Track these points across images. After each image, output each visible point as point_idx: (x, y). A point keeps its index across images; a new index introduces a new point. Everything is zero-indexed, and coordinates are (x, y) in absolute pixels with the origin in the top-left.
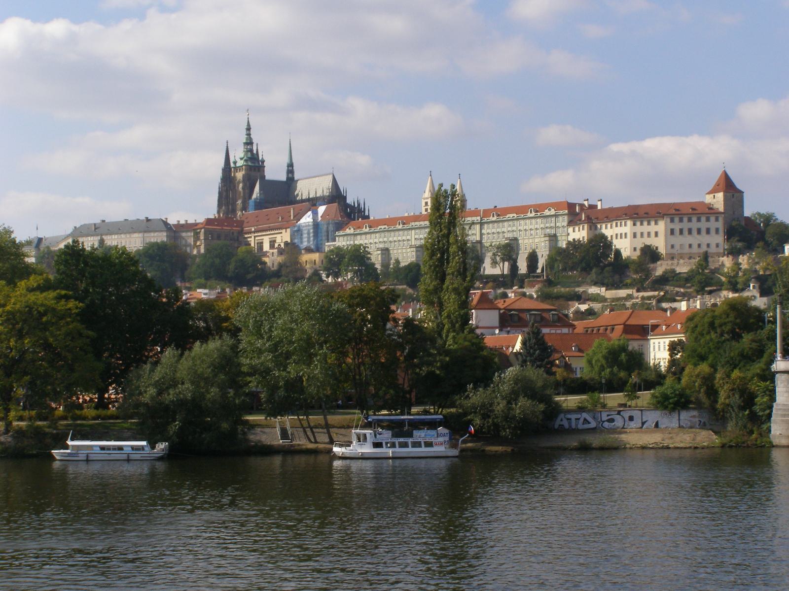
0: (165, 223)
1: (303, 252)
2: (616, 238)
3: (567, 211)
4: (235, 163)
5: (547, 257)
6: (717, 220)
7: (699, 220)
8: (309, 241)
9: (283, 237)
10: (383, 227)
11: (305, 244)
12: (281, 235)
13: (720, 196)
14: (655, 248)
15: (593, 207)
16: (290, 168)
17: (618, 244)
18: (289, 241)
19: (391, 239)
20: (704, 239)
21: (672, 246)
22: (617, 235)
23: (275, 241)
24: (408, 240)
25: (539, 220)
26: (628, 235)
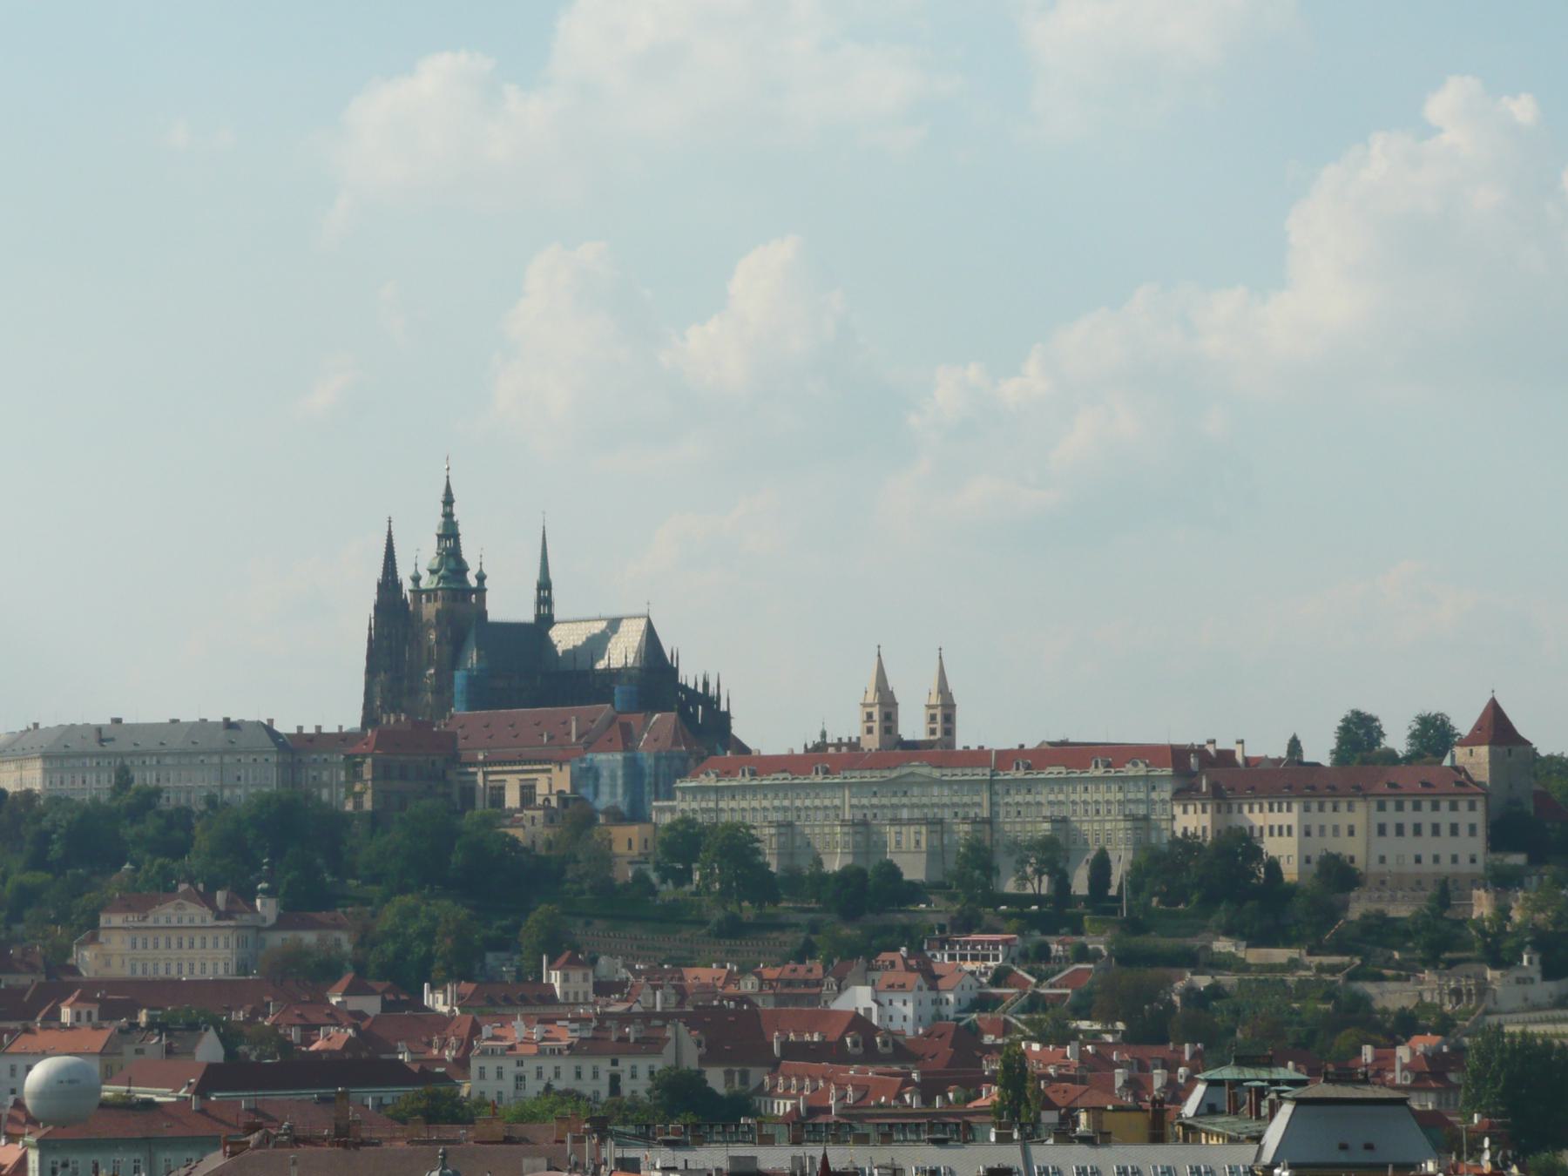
0: (268, 728)
1: (602, 819)
2: (1271, 834)
3: (1170, 769)
4: (416, 579)
5: (1128, 867)
7: (1436, 807)
8: (613, 794)
9: (554, 782)
10: (781, 776)
11: (603, 801)
13: (1483, 751)
14: (1348, 860)
15: (1226, 757)
17: (1272, 847)
18: (568, 791)
19: (798, 803)
20: (1446, 845)
21: (1382, 859)
22: (1271, 828)
23: (533, 787)
24: (836, 807)
25: (1114, 787)
26: (1295, 831)
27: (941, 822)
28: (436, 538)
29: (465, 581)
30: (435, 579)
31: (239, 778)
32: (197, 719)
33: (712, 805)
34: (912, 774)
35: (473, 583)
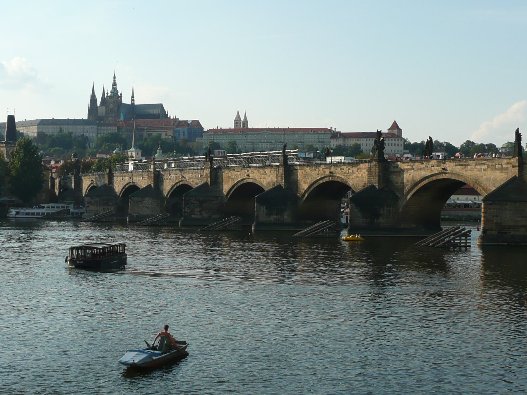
4: (107, 94)
6: (401, 141)
8: (184, 136)
10: (231, 133)
12: (166, 132)
16: (133, 99)
19: (235, 138)
20: (396, 148)
23: (160, 135)
26: (364, 144)
27: (272, 142)
28: (112, 86)
29: (118, 95)
30: (113, 94)
31: (87, 131)
32: (73, 118)
33: (212, 139)
34: (265, 132)
35: (120, 95)
